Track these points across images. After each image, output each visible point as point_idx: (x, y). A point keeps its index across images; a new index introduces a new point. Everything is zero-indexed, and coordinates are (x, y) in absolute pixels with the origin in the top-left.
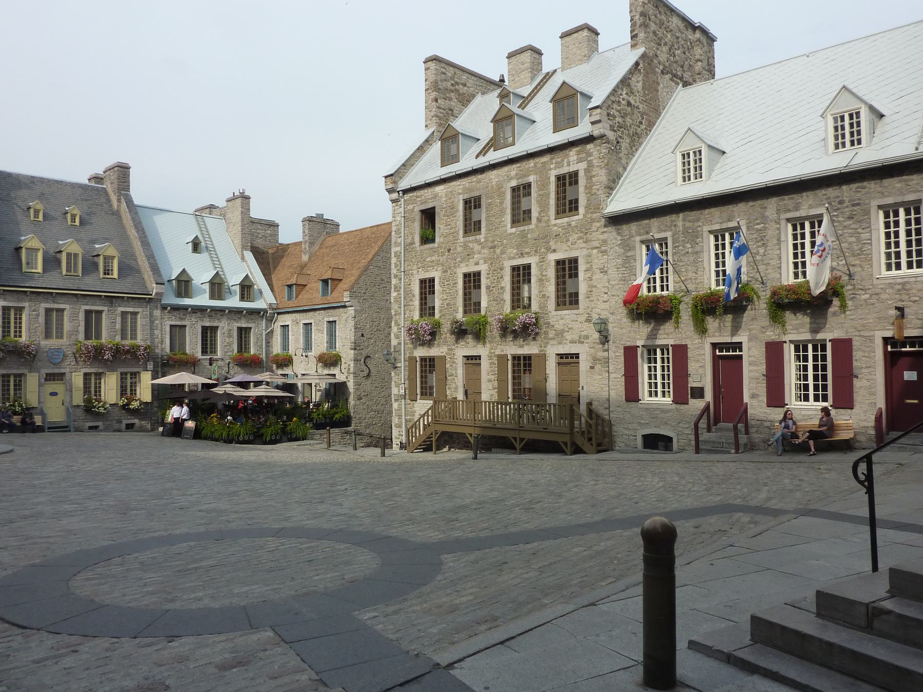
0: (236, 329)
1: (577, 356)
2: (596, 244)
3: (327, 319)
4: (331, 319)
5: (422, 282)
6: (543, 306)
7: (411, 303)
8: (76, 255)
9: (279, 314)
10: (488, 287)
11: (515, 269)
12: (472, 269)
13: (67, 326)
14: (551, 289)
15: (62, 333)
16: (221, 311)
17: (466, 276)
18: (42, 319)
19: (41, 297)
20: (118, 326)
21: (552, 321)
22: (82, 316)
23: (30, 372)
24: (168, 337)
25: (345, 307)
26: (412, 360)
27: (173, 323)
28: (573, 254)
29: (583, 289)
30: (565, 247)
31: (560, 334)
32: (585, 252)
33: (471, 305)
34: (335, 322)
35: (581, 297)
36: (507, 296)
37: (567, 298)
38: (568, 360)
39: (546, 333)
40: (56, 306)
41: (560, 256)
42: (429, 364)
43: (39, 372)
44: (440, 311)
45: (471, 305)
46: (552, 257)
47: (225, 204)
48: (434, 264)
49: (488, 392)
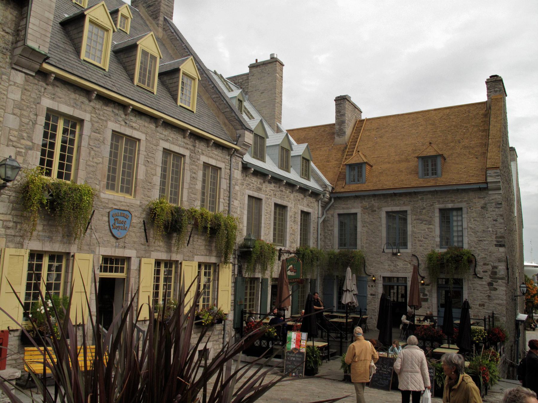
0: (300, 212)
3: (438, 206)
4: (450, 206)
8: (153, 58)
9: (337, 199)
13: (141, 172)
15: (129, 182)
16: (291, 185)
18: (106, 150)
19: (109, 110)
20: (199, 186)
22: (159, 156)
23: (80, 250)
24: (246, 212)
25: (486, 189)
27: (251, 193)
34: (460, 209)
40: (128, 131)
43: (93, 252)
47: (247, 70)
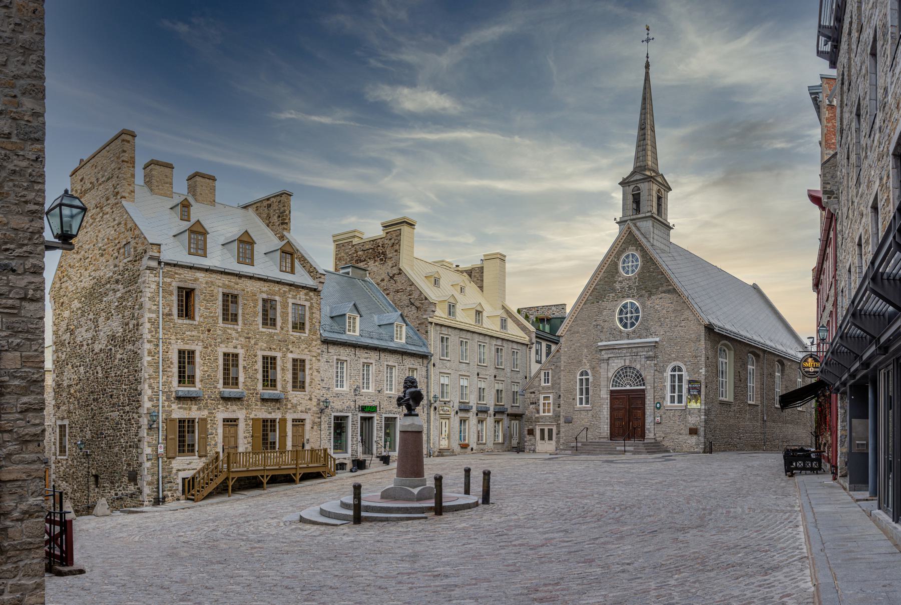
1: (303, 420)
2: (315, 354)
5: (181, 353)
6: (284, 390)
7: (169, 369)
10: (244, 367)
11: (265, 358)
12: (231, 350)
14: (289, 376)
17: (226, 355)
21: (290, 397)
26: (168, 421)
28: (303, 357)
29: (308, 380)
30: (298, 351)
31: (294, 406)
32: (309, 358)
33: (230, 380)
35: (307, 385)
36: (260, 376)
37: (299, 384)
38: (299, 423)
39: (286, 405)
41: (295, 356)
42: (185, 427)
44: (201, 381)
45: (230, 380)
46: (290, 356)
48: (193, 339)
49: (243, 445)
